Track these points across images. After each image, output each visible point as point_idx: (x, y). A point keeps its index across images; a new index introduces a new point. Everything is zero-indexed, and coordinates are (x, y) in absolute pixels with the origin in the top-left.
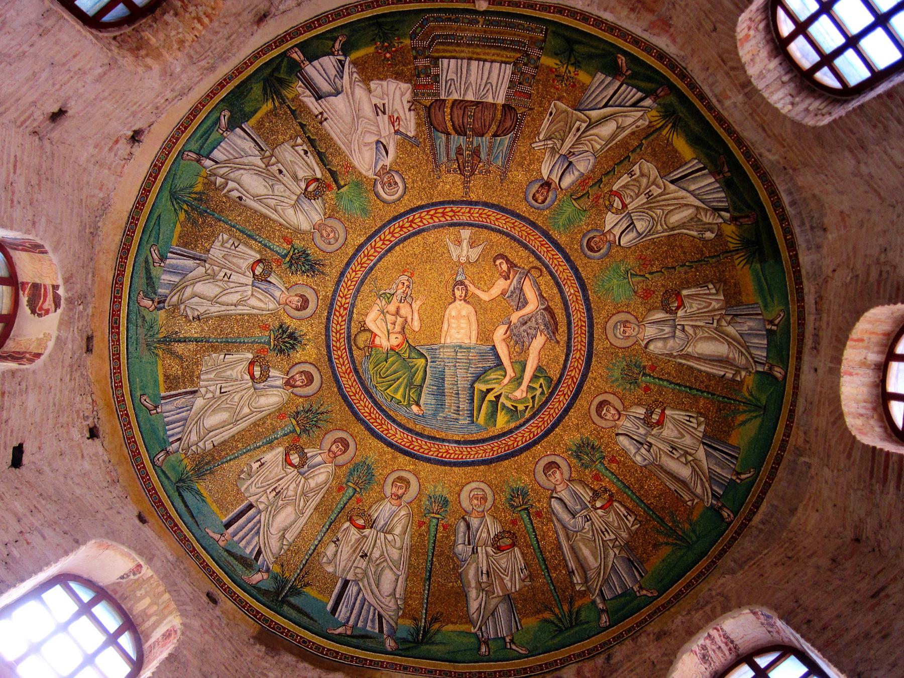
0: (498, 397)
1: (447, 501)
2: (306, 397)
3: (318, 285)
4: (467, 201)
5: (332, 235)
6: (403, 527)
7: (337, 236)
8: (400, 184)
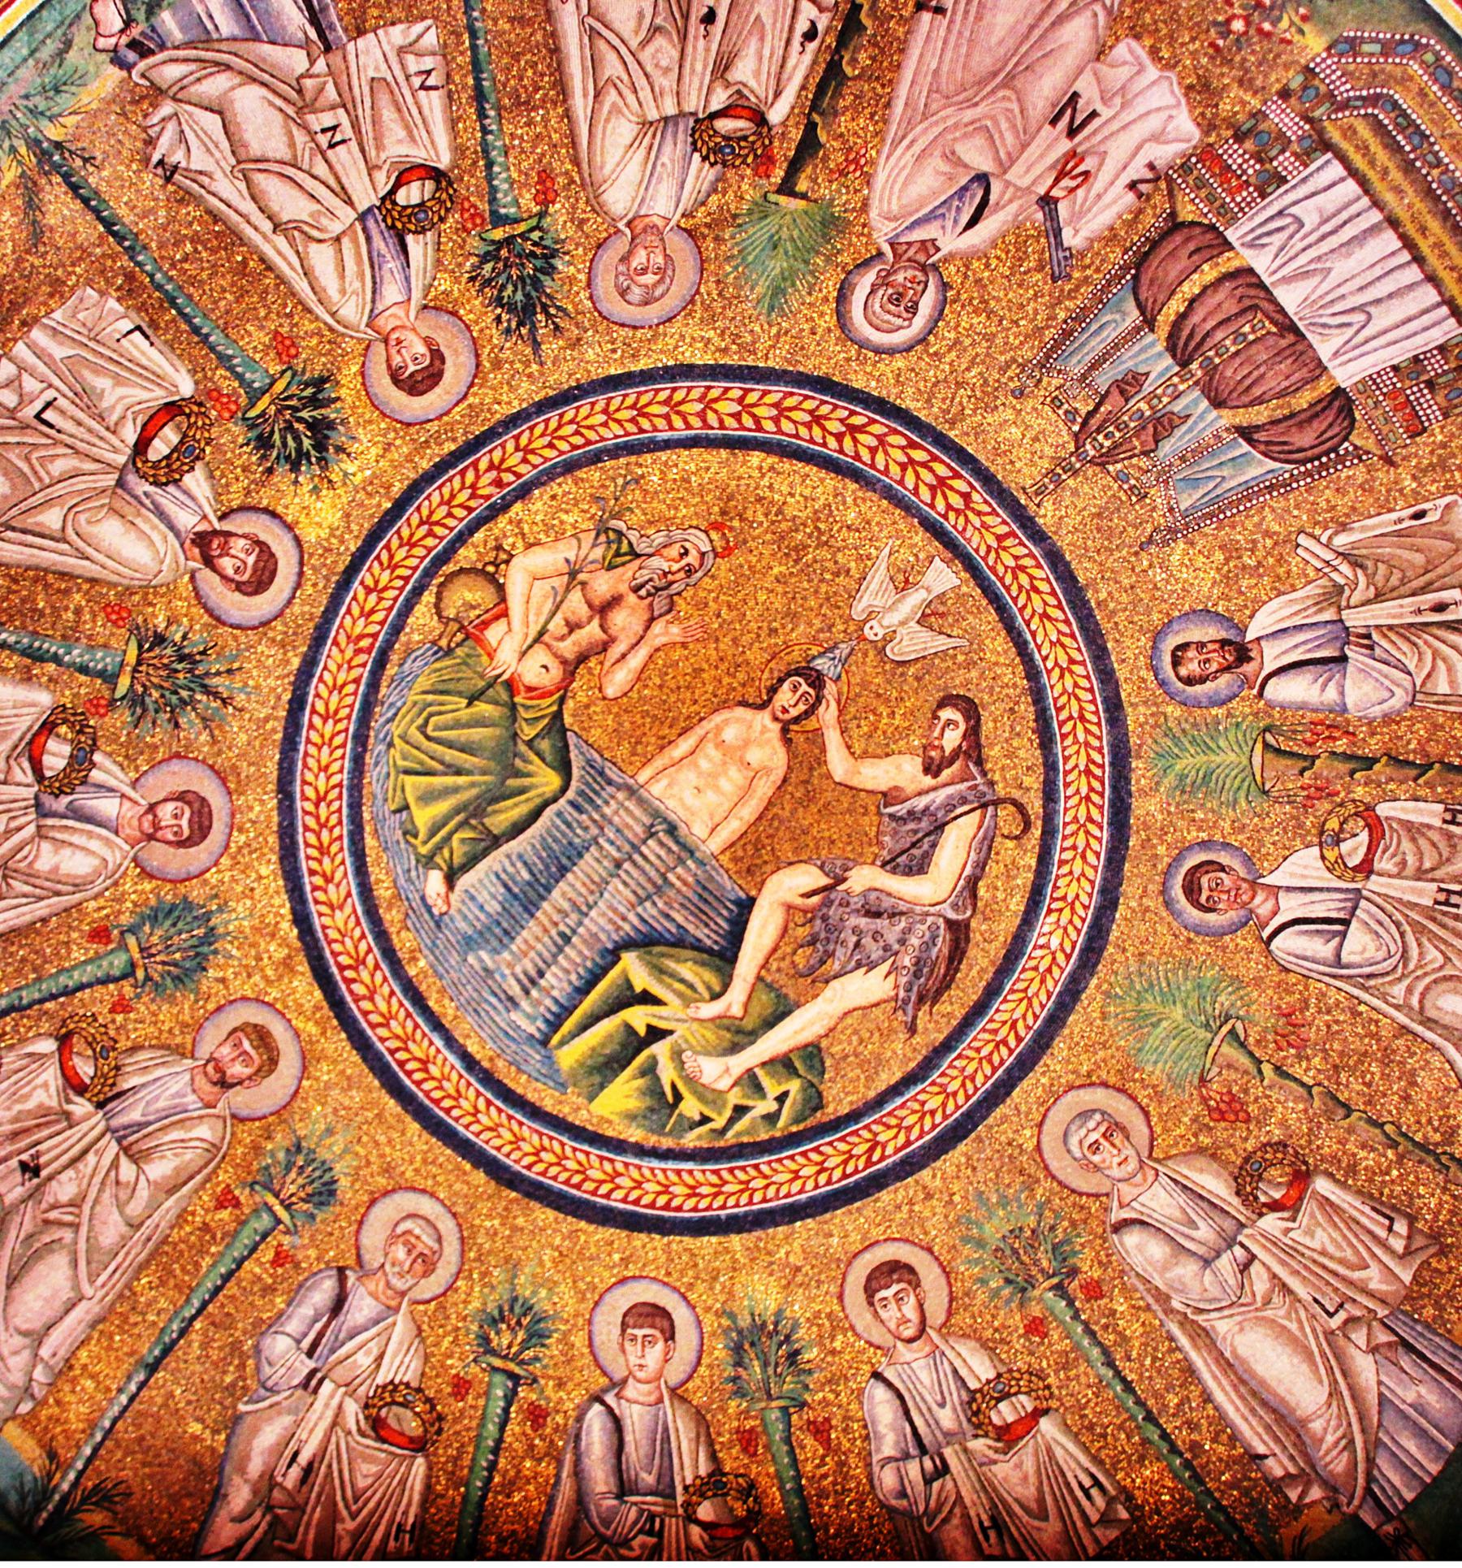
0: (656, 1034)
1: (332, 1193)
2: (209, 612)
3: (497, 365)
4: (1025, 508)
5: (649, 279)
6: (177, 1170)
7: (658, 293)
8: (919, 322)
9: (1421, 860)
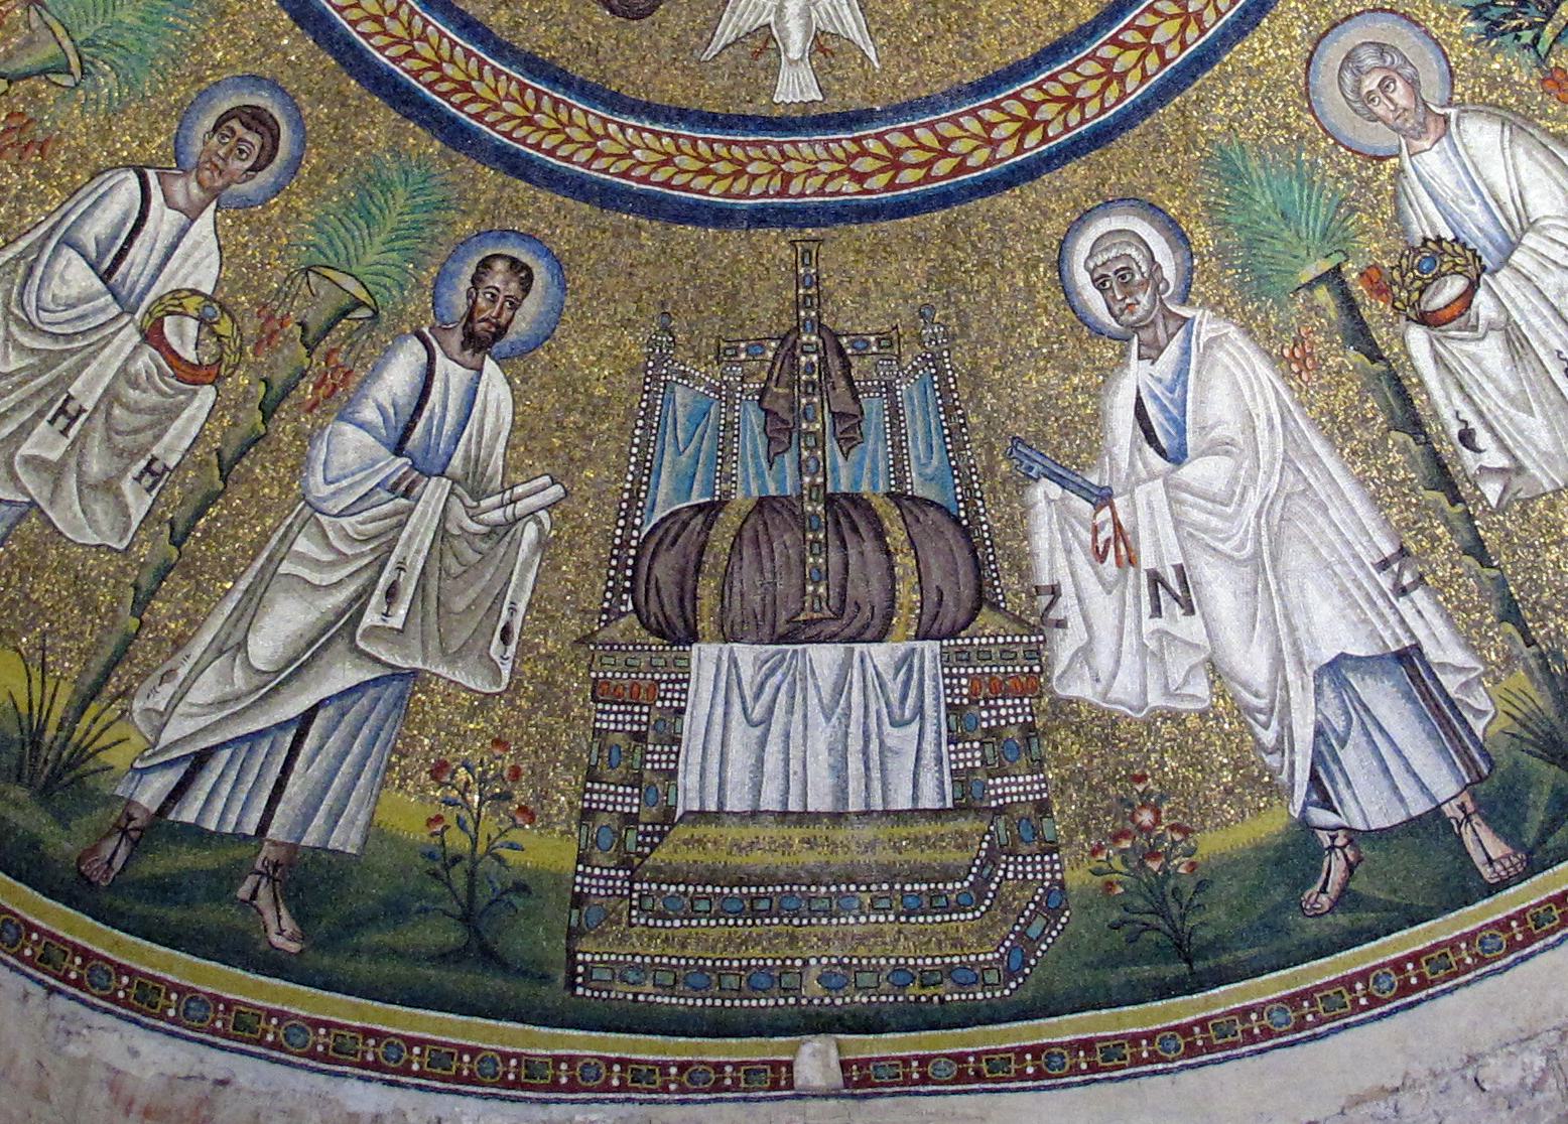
4: (802, 227)
5: (1371, 83)
7: (1348, 77)
8: (1082, 278)
9: (126, 406)
